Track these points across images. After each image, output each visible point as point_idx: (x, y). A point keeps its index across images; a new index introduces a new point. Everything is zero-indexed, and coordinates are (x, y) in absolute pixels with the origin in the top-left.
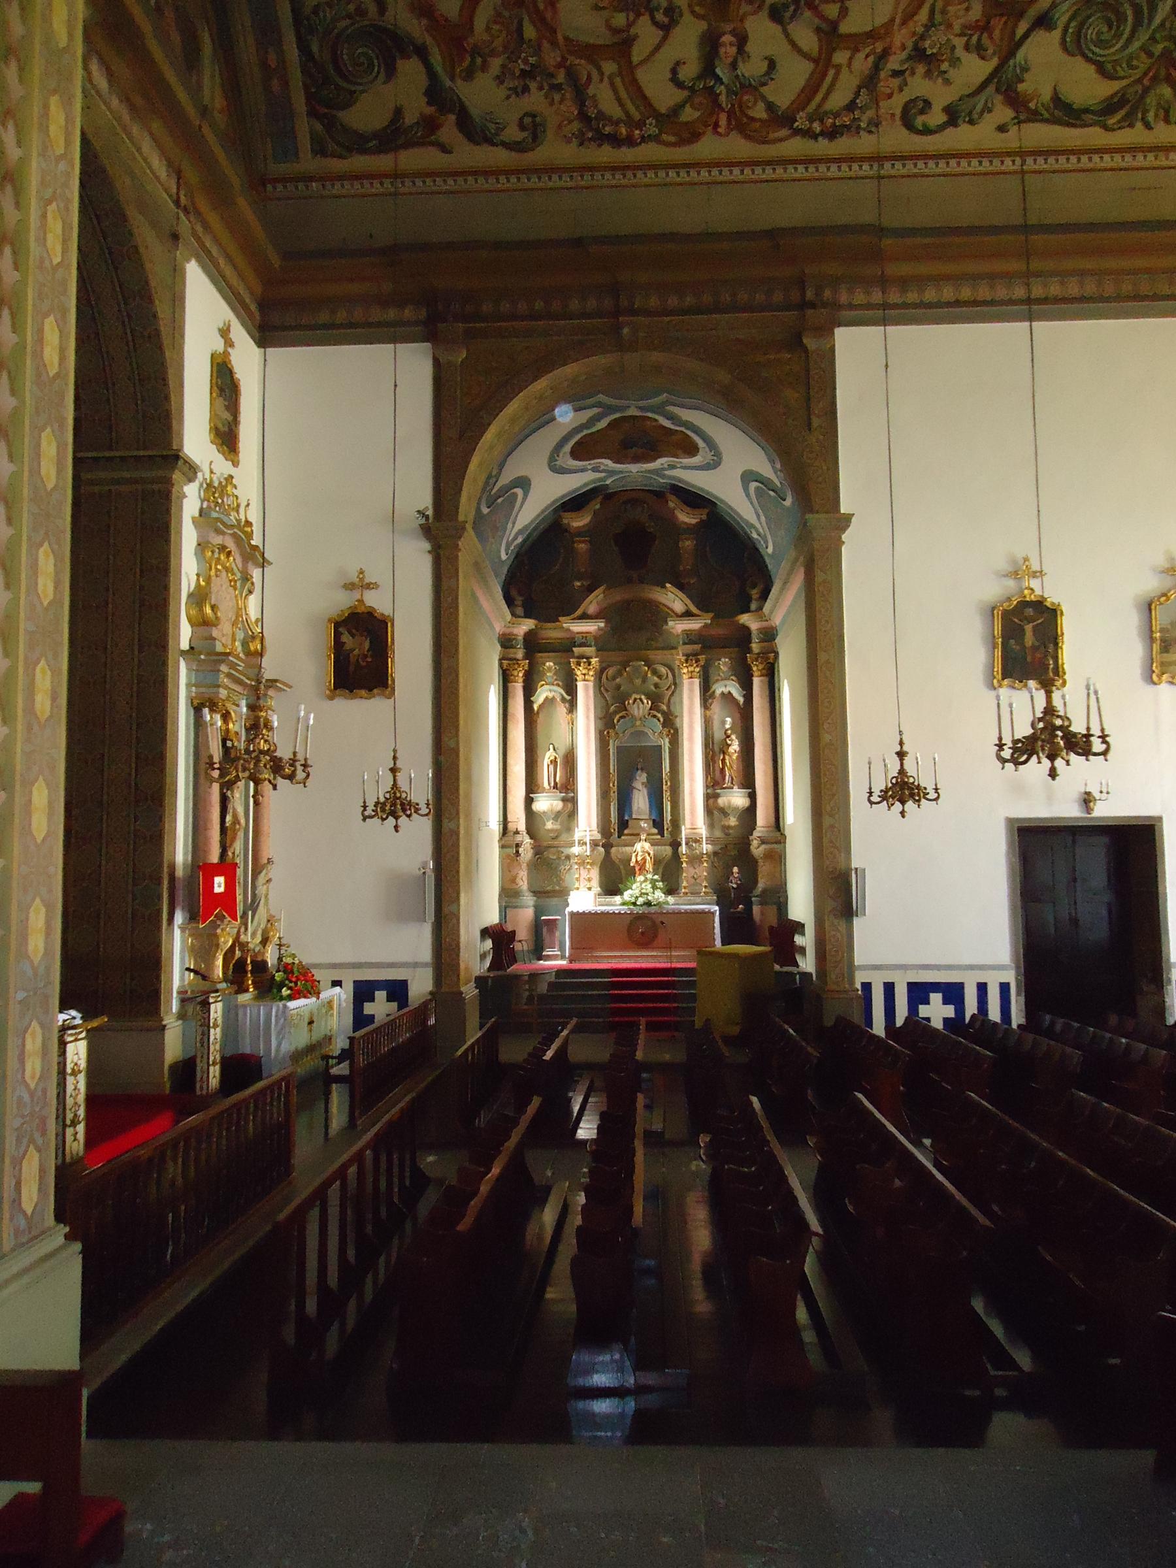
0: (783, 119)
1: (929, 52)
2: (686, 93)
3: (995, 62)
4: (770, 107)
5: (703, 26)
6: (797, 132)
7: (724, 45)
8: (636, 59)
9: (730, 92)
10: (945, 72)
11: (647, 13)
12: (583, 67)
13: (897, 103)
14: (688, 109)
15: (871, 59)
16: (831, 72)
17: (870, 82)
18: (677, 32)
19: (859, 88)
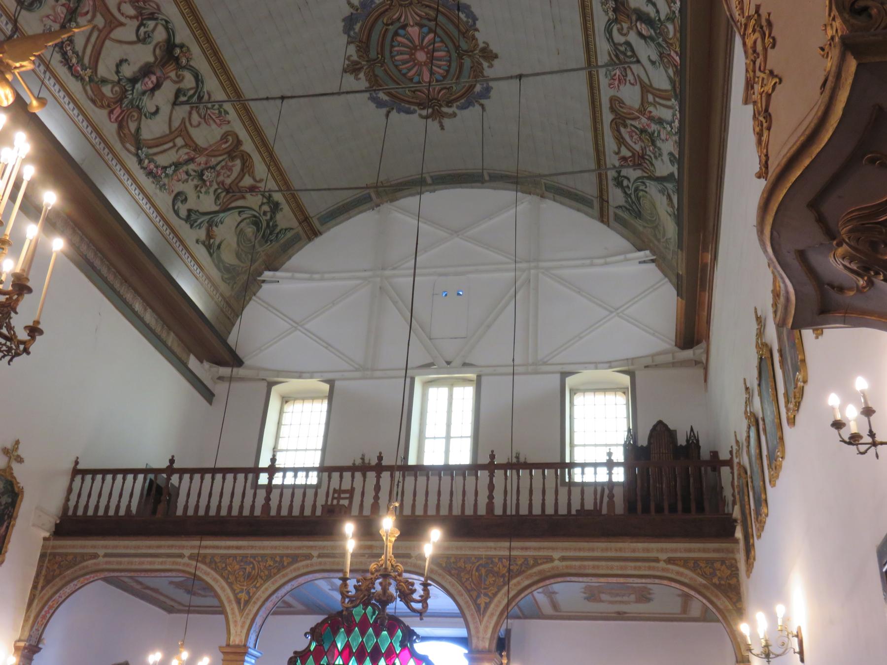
0: (138, 143)
1: (204, 177)
2: (116, 78)
3: (217, 208)
4: (138, 129)
5: (151, 59)
6: (137, 155)
7: (150, 79)
8: (112, 35)
9: (131, 102)
10: (201, 193)
13: (179, 187)
14: (110, 86)
15: (186, 157)
16: (171, 144)
17: (177, 165)
18: (139, 46)
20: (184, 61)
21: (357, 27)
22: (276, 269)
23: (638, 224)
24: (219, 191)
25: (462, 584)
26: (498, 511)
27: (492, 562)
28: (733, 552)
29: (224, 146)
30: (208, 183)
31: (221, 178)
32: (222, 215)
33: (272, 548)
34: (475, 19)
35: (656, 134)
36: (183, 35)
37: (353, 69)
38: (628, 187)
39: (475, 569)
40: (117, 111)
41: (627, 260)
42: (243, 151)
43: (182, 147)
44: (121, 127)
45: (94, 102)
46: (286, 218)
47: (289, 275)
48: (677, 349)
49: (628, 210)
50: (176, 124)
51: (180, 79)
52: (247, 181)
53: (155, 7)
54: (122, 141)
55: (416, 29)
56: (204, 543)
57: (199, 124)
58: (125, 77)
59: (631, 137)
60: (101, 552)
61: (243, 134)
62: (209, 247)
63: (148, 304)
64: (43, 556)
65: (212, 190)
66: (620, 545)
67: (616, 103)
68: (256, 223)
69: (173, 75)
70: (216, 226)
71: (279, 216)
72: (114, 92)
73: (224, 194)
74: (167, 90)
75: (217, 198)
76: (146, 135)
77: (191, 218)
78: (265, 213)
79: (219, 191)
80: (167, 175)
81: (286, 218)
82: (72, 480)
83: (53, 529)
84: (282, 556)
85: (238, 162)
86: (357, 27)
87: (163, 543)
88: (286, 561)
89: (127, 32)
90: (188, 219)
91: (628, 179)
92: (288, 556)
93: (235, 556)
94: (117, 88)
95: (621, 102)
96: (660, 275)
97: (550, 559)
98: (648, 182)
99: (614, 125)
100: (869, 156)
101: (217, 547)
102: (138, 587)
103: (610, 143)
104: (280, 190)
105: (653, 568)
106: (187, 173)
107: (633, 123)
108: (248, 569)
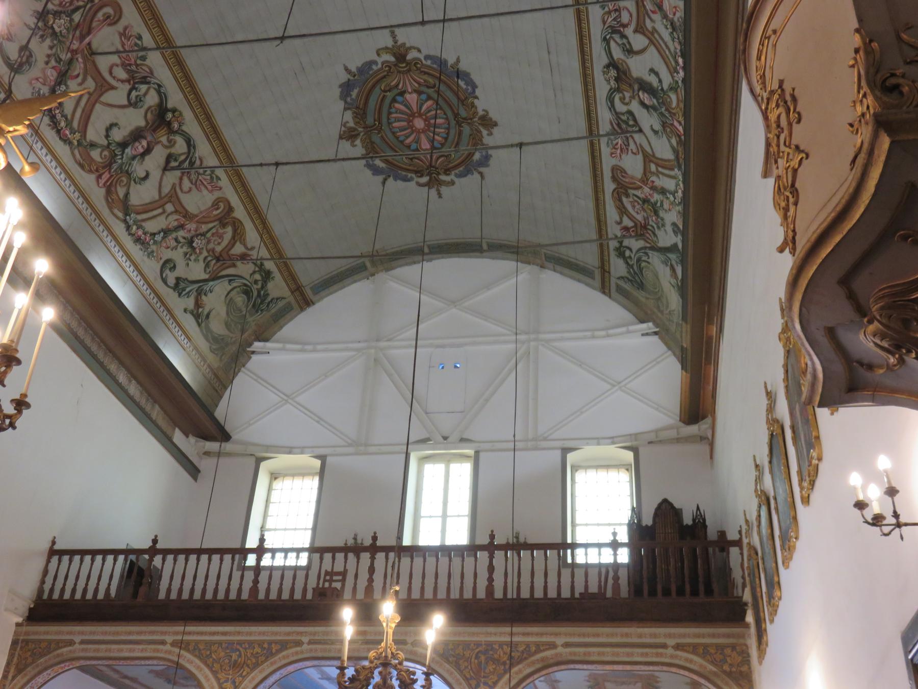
0: (127, 209)
1: (194, 245)
2: (105, 143)
3: (207, 276)
4: (127, 195)
6: (125, 221)
7: (140, 143)
8: (103, 99)
9: (120, 167)
10: (190, 260)
11: (131, 86)
12: (78, 67)
13: (167, 254)
14: (99, 150)
15: (176, 224)
16: (160, 210)
17: (166, 232)
19: (162, 230)
20: (176, 126)
21: (354, 93)
22: (266, 340)
23: (640, 295)
24: (209, 258)
25: (461, 672)
26: (499, 594)
27: (492, 649)
28: (743, 636)
29: (215, 213)
30: (198, 251)
31: (211, 246)
32: (211, 283)
33: (260, 634)
34: (474, 87)
35: (659, 204)
36: (176, 99)
37: (349, 135)
38: (630, 257)
39: (474, 656)
40: (106, 176)
41: (629, 332)
42: (234, 218)
43: (172, 213)
44: (109, 192)
45: (82, 166)
46: (278, 287)
47: (280, 345)
48: (681, 424)
49: (631, 281)
50: (166, 190)
51: (172, 144)
52: (238, 249)
53: (148, 71)
54: (110, 206)
55: (415, 96)
56: (189, 629)
57: (190, 190)
58: (115, 141)
59: (634, 207)
60: (77, 639)
61: (235, 201)
62: (197, 317)
63: (133, 376)
64: (15, 643)
65: (201, 258)
66: (626, 630)
67: (618, 173)
68: (247, 292)
69: (164, 139)
70: (205, 295)
71: (270, 285)
72: (103, 156)
73: (214, 261)
74: (158, 155)
75: (207, 265)
76: (134, 200)
77: (179, 286)
78: (256, 282)
79: (209, 258)
80: (155, 242)
81: (278, 287)
82: (48, 561)
83: (27, 614)
84: (270, 643)
85: (229, 230)
86: (354, 93)
87: (144, 628)
88: (275, 648)
89: (119, 96)
90: (176, 287)
91: (631, 250)
92: (276, 642)
93: (220, 643)
94: (106, 153)
95: (623, 171)
96: (663, 348)
97: (553, 646)
98: (650, 253)
99: (616, 195)
100: (902, 232)
101: (202, 633)
102: (116, 676)
103: (612, 213)
104: (272, 259)
105: (661, 655)
106: (176, 240)
107: (636, 192)
108: (234, 656)
